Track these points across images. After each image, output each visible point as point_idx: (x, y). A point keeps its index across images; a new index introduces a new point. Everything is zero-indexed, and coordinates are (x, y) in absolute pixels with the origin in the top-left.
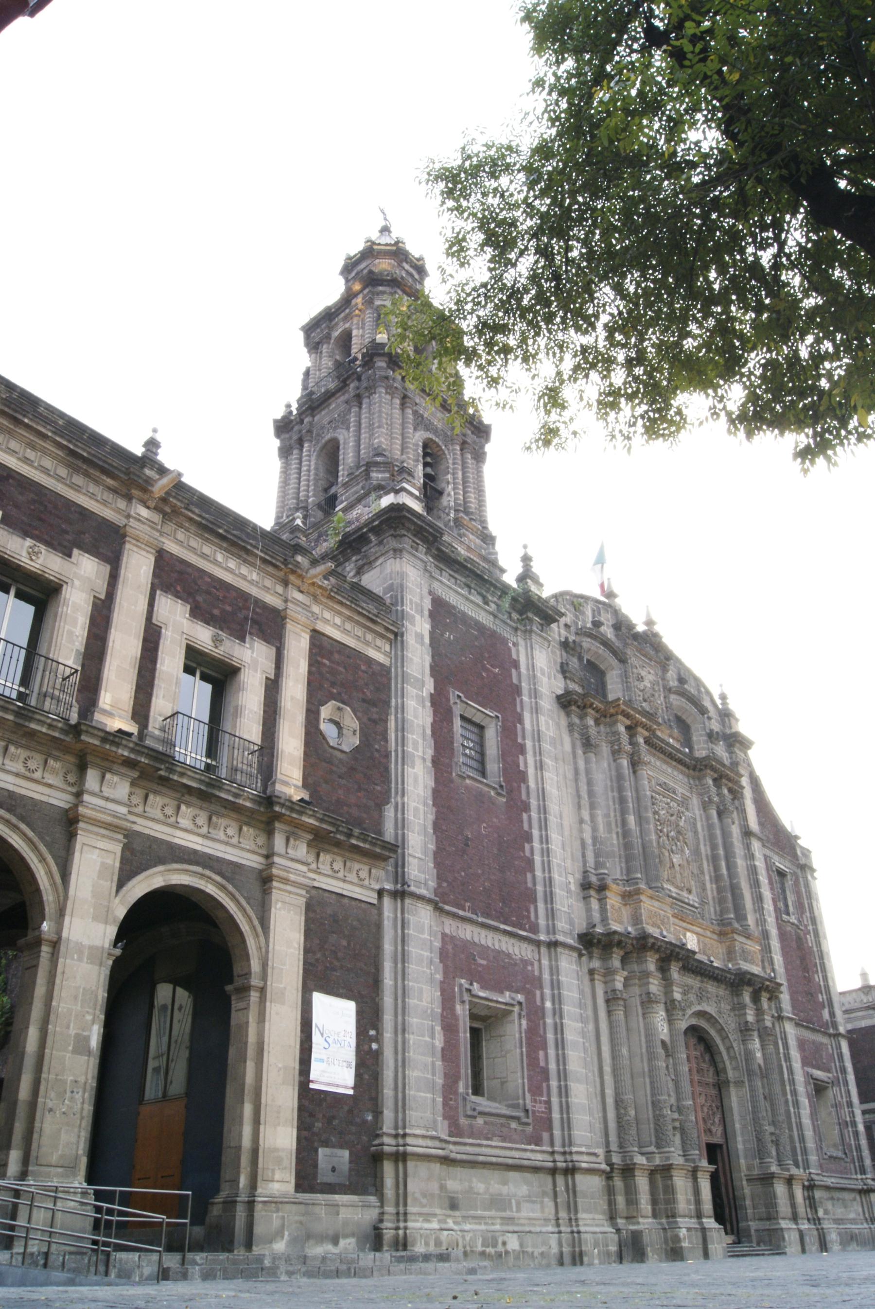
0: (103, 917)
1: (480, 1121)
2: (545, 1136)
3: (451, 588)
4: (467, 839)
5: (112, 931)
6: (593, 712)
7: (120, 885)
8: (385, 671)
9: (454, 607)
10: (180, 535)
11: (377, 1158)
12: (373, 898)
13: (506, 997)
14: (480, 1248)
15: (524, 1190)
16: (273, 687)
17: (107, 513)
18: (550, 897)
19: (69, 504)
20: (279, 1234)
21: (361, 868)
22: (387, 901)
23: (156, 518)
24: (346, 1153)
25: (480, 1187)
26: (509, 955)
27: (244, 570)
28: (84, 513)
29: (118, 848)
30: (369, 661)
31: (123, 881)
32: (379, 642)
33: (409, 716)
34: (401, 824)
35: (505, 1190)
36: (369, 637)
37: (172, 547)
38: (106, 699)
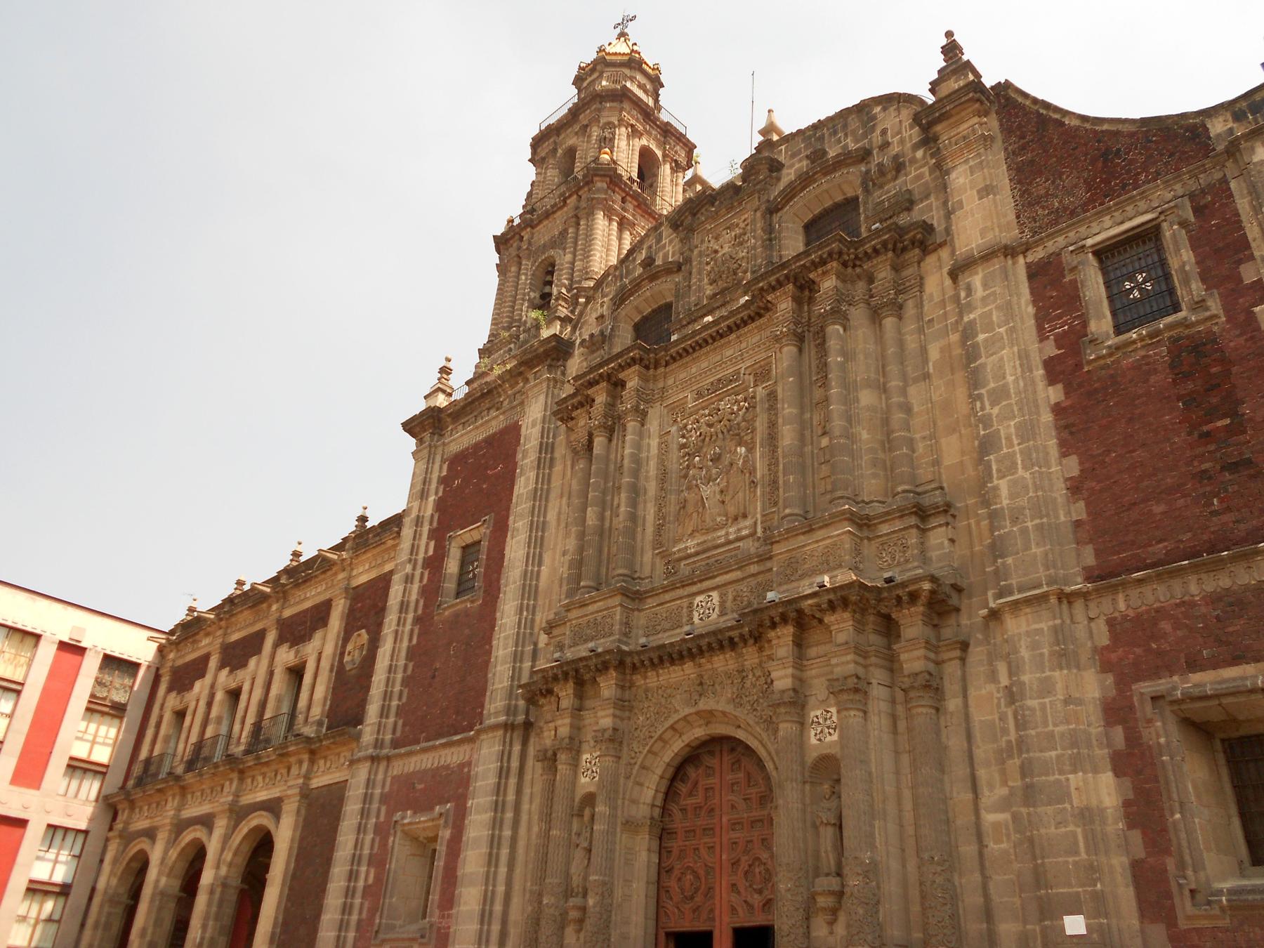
3: (462, 435)
4: (436, 670)
6: (579, 411)
9: (467, 449)
26: (447, 767)
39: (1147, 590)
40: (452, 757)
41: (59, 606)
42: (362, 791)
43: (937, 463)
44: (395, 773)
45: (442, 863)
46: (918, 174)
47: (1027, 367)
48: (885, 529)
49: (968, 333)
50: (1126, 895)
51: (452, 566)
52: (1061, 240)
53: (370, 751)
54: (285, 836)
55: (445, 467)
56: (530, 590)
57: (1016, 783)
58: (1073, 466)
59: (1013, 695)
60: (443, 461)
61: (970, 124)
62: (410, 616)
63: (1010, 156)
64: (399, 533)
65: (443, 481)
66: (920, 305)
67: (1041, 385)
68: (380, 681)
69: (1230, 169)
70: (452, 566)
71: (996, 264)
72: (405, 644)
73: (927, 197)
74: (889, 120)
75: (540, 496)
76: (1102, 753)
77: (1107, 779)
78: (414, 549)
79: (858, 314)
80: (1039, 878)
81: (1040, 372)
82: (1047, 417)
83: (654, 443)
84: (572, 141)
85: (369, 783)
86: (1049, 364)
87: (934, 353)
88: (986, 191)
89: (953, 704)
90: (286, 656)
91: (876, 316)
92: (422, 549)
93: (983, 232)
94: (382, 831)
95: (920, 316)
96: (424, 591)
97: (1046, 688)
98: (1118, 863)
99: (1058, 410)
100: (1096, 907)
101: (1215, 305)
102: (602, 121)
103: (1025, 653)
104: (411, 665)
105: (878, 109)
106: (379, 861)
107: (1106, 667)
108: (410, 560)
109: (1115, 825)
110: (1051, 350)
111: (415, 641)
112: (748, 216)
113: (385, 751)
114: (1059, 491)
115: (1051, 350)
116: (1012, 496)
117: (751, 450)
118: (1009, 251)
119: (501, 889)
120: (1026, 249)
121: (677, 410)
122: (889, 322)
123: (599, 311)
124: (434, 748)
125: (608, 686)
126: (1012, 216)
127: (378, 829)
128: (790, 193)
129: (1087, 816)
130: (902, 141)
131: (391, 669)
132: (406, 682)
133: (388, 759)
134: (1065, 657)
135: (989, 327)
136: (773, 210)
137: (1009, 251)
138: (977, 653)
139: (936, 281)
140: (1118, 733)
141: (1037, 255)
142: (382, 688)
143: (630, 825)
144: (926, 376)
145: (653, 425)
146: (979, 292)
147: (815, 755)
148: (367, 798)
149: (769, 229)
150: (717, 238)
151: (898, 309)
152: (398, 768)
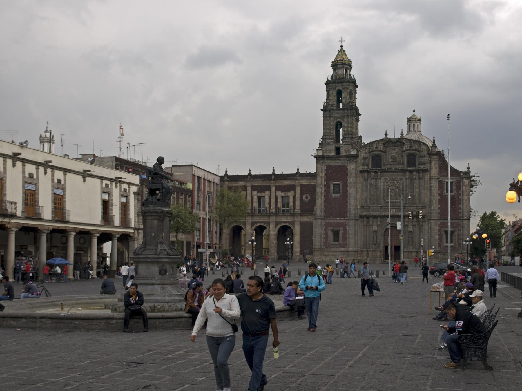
0: (274, 231)
1: (331, 246)
2: (345, 247)
5: (276, 232)
7: (276, 227)
8: (315, 185)
10: (278, 182)
11: (312, 251)
12: (312, 220)
13: (339, 228)
14: (328, 260)
15: (340, 254)
16: (294, 197)
17: (268, 184)
18: (350, 211)
19: (264, 186)
20: (297, 259)
21: (309, 217)
22: (314, 220)
23: (274, 182)
24: (308, 251)
25: (331, 254)
27: (288, 182)
28: (266, 186)
29: (275, 224)
30: (312, 185)
31: (276, 227)
32: (313, 181)
33: (318, 192)
34: (317, 209)
35: (336, 254)
36: (311, 181)
37: (277, 184)
38: (272, 208)
39: (444, 220)
40: (342, 221)
41: (213, 175)
42: (320, 224)
43: (424, 201)
44: (326, 221)
45: (342, 236)
46: (427, 159)
47: (437, 194)
48: (419, 208)
49: (431, 187)
50: (438, 245)
51: (332, 188)
52: (443, 179)
53: (320, 218)
54: (297, 229)
55: (326, 167)
56: (355, 198)
57: (429, 235)
58: (439, 206)
59: (430, 228)
60: (325, 166)
61: (435, 157)
62: (323, 195)
63: (440, 164)
64: (316, 178)
65: (325, 170)
66: (424, 179)
67: (438, 196)
68: (319, 206)
69: (461, 179)
70: (332, 188)
71: (435, 179)
72: (323, 200)
73: (428, 164)
74: (423, 147)
75: (355, 183)
76: (438, 234)
77: (438, 236)
78: (322, 183)
79: (417, 177)
80: (431, 243)
81: (438, 195)
82: (438, 200)
83: (382, 183)
84: (341, 88)
85: (321, 223)
86: (439, 194)
87: (426, 186)
88: (436, 168)
89: (424, 227)
90: (280, 194)
91: (419, 179)
92: (323, 183)
93: (435, 174)
94: (326, 230)
95: (424, 181)
96: (325, 191)
97: (434, 228)
98: (437, 243)
99: (439, 199)
100: (435, 246)
101: (456, 194)
102: (350, 88)
103: (432, 224)
104: (325, 204)
105: (422, 144)
106: (326, 234)
107: (439, 226)
108: (321, 185)
109: (438, 240)
110: (440, 192)
111: (325, 200)
112: (397, 150)
113: (323, 218)
114: (438, 209)
115: (440, 192)
116: (433, 208)
117: (399, 190)
118: (437, 178)
119: (356, 240)
120: (439, 178)
121: (386, 179)
122: (421, 181)
123: (364, 152)
124: (337, 219)
125: (379, 219)
126: (438, 173)
127: (324, 229)
128: (406, 150)
129: (436, 239)
130: (425, 152)
131: (321, 204)
132: (324, 206)
133: (324, 219)
134: (436, 225)
135: (434, 187)
136: (403, 152)
137: (437, 178)
138: (427, 222)
139: (427, 177)
140: (439, 232)
141: (440, 179)
142: (320, 207)
143: (381, 235)
144: (424, 189)
145: (382, 181)
146: (433, 182)
147: (409, 231)
148: (321, 225)
149: (402, 155)
150: (392, 150)
151: (422, 178)
152: (327, 221)
